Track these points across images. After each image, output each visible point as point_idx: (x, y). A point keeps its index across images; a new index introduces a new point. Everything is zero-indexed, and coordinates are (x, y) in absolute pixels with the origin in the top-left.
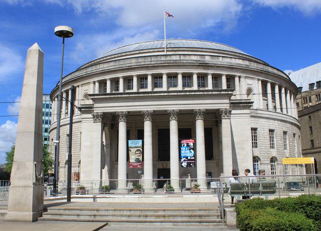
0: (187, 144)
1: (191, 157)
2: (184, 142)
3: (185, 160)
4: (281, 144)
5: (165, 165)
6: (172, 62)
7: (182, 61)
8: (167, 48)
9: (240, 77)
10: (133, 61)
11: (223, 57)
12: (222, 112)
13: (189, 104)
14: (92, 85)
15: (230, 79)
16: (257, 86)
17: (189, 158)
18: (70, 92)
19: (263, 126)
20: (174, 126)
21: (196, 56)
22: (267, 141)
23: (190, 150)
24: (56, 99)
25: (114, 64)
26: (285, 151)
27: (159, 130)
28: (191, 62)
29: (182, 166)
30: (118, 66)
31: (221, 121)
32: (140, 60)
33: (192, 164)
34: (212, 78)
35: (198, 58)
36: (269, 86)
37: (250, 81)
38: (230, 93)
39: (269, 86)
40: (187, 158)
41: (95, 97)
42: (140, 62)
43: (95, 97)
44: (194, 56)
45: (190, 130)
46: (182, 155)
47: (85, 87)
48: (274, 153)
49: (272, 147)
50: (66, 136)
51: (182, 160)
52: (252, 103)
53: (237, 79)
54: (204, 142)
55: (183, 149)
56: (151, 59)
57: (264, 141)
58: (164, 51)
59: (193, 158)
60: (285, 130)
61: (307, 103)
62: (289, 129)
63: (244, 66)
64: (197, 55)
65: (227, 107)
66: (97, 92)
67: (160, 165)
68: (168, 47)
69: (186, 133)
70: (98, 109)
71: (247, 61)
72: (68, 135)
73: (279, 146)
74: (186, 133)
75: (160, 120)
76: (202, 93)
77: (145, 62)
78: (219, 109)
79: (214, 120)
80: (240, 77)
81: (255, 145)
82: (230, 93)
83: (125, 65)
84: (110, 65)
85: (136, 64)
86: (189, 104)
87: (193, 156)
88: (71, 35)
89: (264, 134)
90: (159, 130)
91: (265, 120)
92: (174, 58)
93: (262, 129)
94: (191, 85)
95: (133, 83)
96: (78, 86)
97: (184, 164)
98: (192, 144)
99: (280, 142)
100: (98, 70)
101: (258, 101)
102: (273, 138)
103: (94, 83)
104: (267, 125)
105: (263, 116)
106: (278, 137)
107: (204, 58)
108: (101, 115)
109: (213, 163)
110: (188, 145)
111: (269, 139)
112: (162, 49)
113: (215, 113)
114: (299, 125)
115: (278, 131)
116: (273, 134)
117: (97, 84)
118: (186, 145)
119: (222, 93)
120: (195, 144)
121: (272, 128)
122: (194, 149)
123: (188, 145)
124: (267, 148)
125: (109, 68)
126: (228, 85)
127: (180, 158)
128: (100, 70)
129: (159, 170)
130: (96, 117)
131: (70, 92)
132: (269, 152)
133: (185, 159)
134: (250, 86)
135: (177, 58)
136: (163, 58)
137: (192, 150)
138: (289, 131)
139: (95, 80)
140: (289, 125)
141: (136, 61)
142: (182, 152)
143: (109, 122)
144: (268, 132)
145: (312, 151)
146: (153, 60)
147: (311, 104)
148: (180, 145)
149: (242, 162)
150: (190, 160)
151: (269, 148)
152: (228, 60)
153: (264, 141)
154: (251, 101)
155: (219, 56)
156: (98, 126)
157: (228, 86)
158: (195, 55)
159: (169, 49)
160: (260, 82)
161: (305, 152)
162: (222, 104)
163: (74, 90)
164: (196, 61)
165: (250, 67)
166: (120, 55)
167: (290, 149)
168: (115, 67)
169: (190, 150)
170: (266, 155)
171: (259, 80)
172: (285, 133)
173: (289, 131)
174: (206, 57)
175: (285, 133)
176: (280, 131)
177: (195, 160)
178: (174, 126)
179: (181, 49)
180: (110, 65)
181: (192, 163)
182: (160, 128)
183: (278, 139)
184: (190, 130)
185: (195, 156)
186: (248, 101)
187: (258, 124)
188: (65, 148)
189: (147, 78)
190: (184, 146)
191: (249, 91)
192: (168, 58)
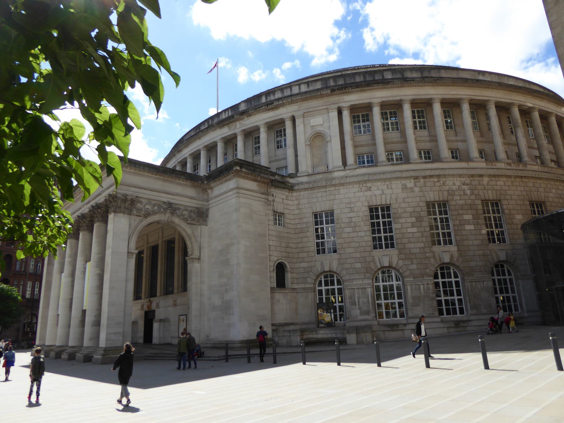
9: (293, 119)
21: (227, 113)
22: (363, 234)
37: (317, 121)
60: (433, 196)
73: (405, 241)
89: (353, 220)
91: (356, 188)
106: (403, 220)
111: (369, 228)
115: (403, 205)
121: (377, 202)
132: (368, 259)
134: (319, 129)
151: (369, 249)
170: (358, 265)
183: (405, 226)
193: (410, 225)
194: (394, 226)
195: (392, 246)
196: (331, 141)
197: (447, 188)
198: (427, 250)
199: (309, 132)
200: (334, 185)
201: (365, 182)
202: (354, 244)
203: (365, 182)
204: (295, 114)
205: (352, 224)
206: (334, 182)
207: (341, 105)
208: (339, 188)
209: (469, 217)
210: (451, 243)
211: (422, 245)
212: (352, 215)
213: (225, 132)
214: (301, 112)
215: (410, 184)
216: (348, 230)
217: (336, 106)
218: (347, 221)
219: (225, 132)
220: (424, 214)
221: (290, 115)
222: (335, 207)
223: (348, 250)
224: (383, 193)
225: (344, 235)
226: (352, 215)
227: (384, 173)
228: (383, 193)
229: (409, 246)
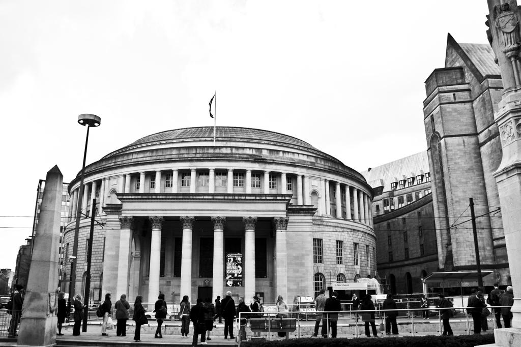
0: (234, 259)
1: (238, 274)
2: (230, 256)
3: (230, 278)
4: (351, 259)
5: (207, 282)
6: (221, 155)
7: (234, 156)
8: (216, 137)
9: (303, 177)
10: (174, 152)
11: (284, 152)
12: (276, 220)
13: (237, 211)
14: (122, 179)
15: (291, 178)
16: (323, 189)
17: (236, 276)
18: (94, 185)
19: (329, 238)
20: (218, 236)
21: (251, 150)
22: (333, 255)
23: (237, 265)
24: (75, 193)
25: (151, 155)
26: (356, 267)
27: (201, 239)
28: (245, 156)
29: (227, 285)
30: (155, 158)
31: (276, 232)
32: (182, 151)
33: (238, 283)
34: (270, 177)
35: (254, 152)
36: (338, 187)
37: (315, 182)
38: (287, 198)
39: (338, 187)
40: (233, 275)
41: (124, 197)
42: (183, 154)
43: (124, 197)
44: (248, 149)
45: (240, 239)
46: (228, 272)
47: (113, 182)
48: (342, 269)
49: (340, 261)
50: (85, 240)
51: (228, 278)
52: (317, 209)
53: (299, 179)
54: (254, 257)
55: (229, 264)
56: (196, 151)
57: (330, 255)
58: (212, 141)
59: (241, 276)
61: (388, 205)
62: (361, 240)
63: (308, 163)
64: (253, 148)
65: (283, 215)
66: (127, 191)
67: (201, 283)
68: (218, 136)
69: (234, 245)
70: (127, 212)
71: (313, 158)
72: (87, 240)
73: (347, 261)
74: (234, 245)
75: (203, 228)
76: (254, 198)
77: (188, 154)
78: (273, 218)
79: (267, 230)
80: (303, 177)
81: (318, 259)
82: (287, 198)
83: (163, 157)
84: (146, 155)
85: (177, 156)
86: (237, 211)
87: (240, 273)
88: (96, 124)
89: (331, 246)
90: (201, 239)
92: (224, 151)
93: (328, 241)
94: (242, 184)
95: (172, 179)
96: (104, 179)
97: (230, 283)
98: (239, 259)
99: (350, 256)
100: (130, 161)
101: (323, 207)
102: (341, 251)
103: (125, 176)
104: (334, 236)
105: (330, 224)
107: (262, 152)
108: (130, 219)
109: (265, 282)
110: (235, 260)
111: (335, 252)
112: (210, 139)
113: (270, 221)
114: (375, 235)
115: (347, 243)
116: (341, 247)
117: (128, 178)
118: (232, 259)
119: (278, 198)
120: (243, 259)
121: (340, 239)
122: (242, 265)
123: (235, 260)
124: (333, 263)
125: (144, 159)
126: (288, 185)
127: (225, 275)
128: (133, 160)
129: (200, 288)
130: (124, 222)
131: (94, 185)
132: (336, 269)
133: (230, 276)
134: (315, 188)
135: (228, 151)
136: (211, 151)
137: (239, 267)
138: (361, 242)
139: (125, 173)
140: (360, 234)
141: (178, 152)
142: (228, 268)
143: (141, 229)
144: (335, 244)
145: (391, 265)
146: (198, 152)
147: (392, 207)
148: (226, 260)
149: (302, 281)
150: (237, 278)
151: (336, 263)
152: (290, 156)
153: (330, 255)
154: (314, 207)
155: (280, 151)
156: (126, 234)
157: (289, 188)
158: (250, 148)
159: (220, 139)
160: (327, 184)
161: (379, 266)
162: (277, 211)
163: (99, 183)
164: (251, 155)
165: (316, 165)
166: (158, 143)
167: (361, 264)
168: (152, 158)
169: (237, 265)
171: (326, 180)
172: (356, 244)
173: (361, 242)
174: (263, 150)
175: (356, 244)
176: (350, 243)
177: (243, 278)
178: (218, 236)
179: (234, 139)
180: (146, 155)
181: (239, 282)
182: (202, 237)
183: (347, 254)
184: (240, 239)
185: (243, 273)
186: (310, 207)
187: (324, 235)
188: (84, 256)
189: (189, 174)
190: (230, 260)
191: (314, 193)
192: (217, 151)
193: (348, 253)
194: (343, 253)
195: (341, 263)
196: (321, 198)
197: (358, 237)
198: (353, 267)
199: (311, 190)
200: (324, 225)
201: (336, 227)
202: (330, 260)
203: (336, 227)
204: (305, 175)
205: (330, 249)
206: (324, 223)
207: (326, 178)
208: (325, 227)
209: (363, 253)
210: (357, 264)
211: (351, 264)
212: (330, 243)
213: (257, 167)
214: (308, 175)
215: (350, 232)
216: (328, 251)
217: (325, 178)
218: (328, 246)
219: (257, 167)
220: (353, 249)
221: (303, 174)
222: (323, 238)
223: (328, 263)
224: (341, 235)
225: (327, 254)
226: (330, 243)
227: (338, 223)
228: (341, 235)
229: (348, 264)
